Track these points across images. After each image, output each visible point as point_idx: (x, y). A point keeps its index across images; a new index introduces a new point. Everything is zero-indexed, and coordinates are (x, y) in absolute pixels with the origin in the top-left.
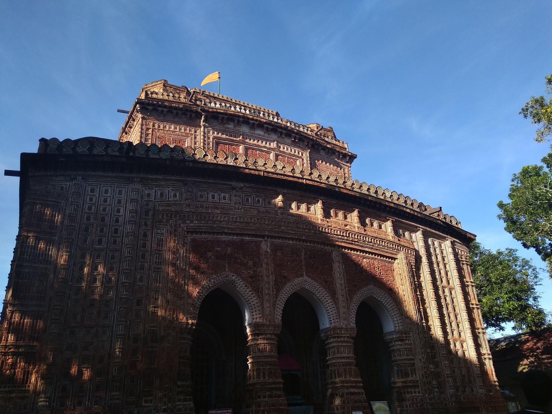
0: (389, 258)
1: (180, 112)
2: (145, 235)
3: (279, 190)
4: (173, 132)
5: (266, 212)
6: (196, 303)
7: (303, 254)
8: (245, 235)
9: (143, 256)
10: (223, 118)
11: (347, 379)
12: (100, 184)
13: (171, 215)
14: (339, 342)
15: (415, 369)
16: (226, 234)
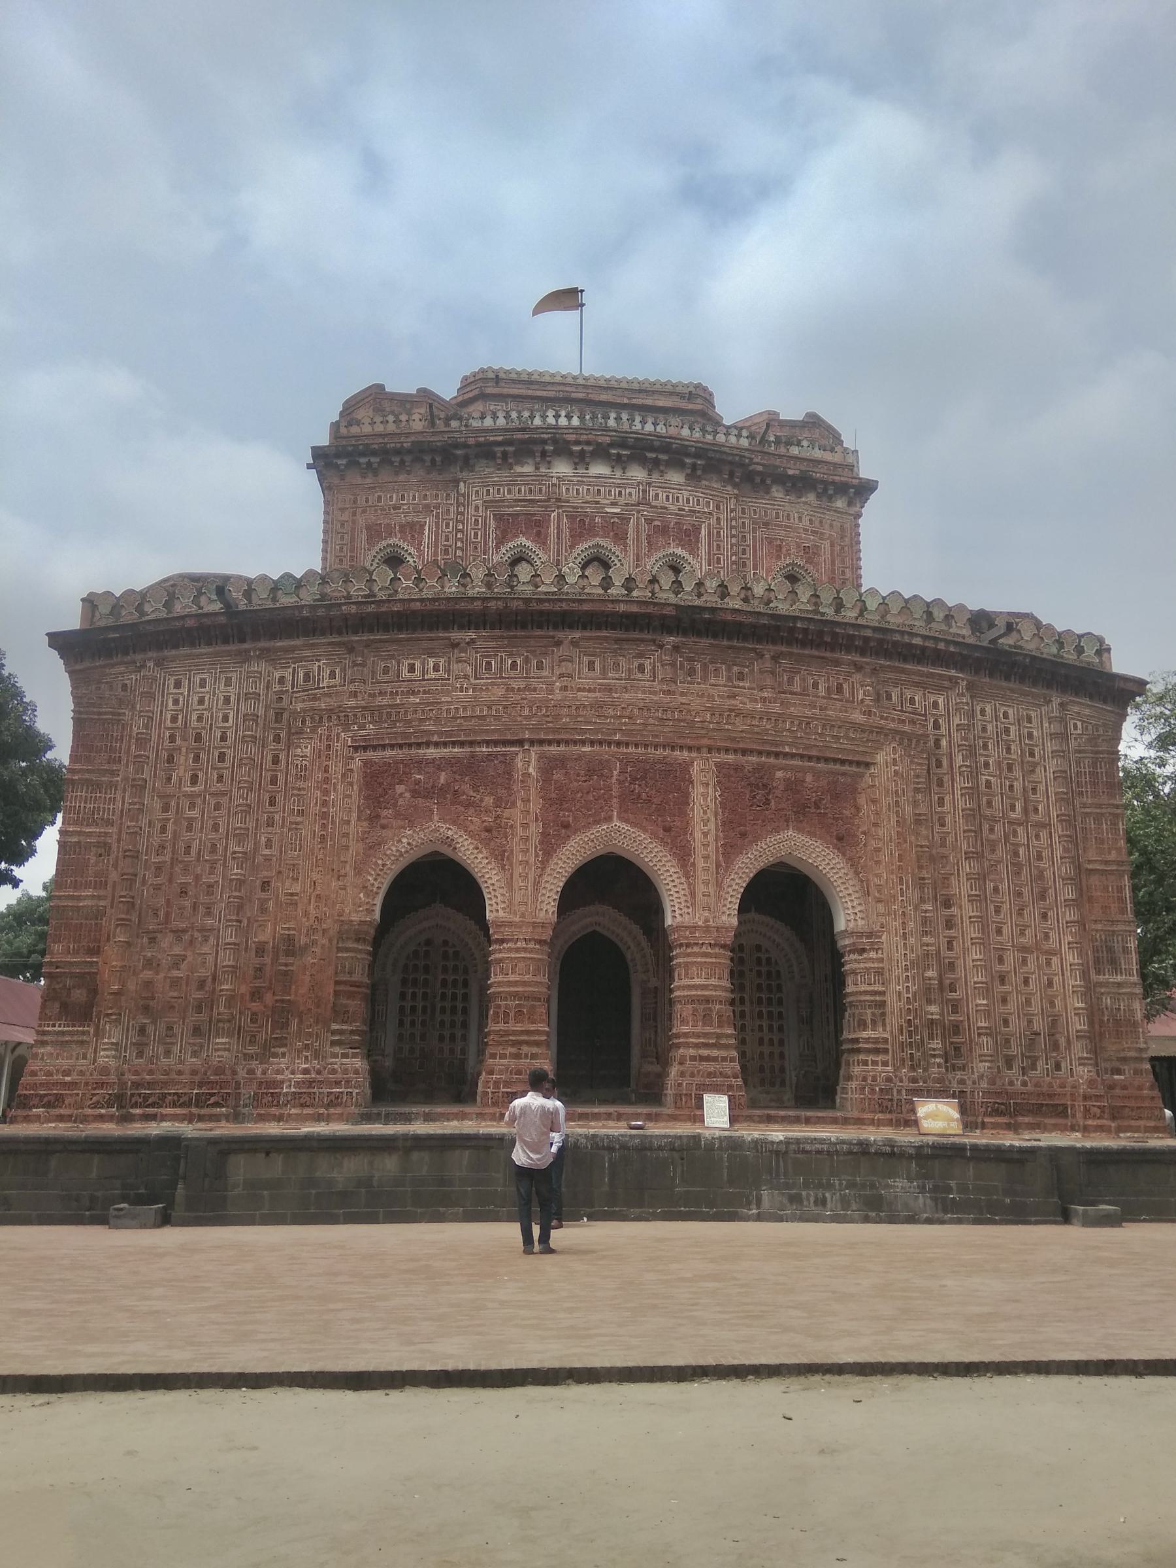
0: (851, 762)
1: (408, 458)
2: (276, 760)
3: (560, 635)
4: (396, 508)
6: (373, 885)
7: (615, 773)
8: (479, 743)
9: (272, 802)
10: (505, 455)
11: (698, 1029)
12: (190, 671)
13: (321, 718)
14: (689, 955)
15: (883, 1014)
16: (437, 745)
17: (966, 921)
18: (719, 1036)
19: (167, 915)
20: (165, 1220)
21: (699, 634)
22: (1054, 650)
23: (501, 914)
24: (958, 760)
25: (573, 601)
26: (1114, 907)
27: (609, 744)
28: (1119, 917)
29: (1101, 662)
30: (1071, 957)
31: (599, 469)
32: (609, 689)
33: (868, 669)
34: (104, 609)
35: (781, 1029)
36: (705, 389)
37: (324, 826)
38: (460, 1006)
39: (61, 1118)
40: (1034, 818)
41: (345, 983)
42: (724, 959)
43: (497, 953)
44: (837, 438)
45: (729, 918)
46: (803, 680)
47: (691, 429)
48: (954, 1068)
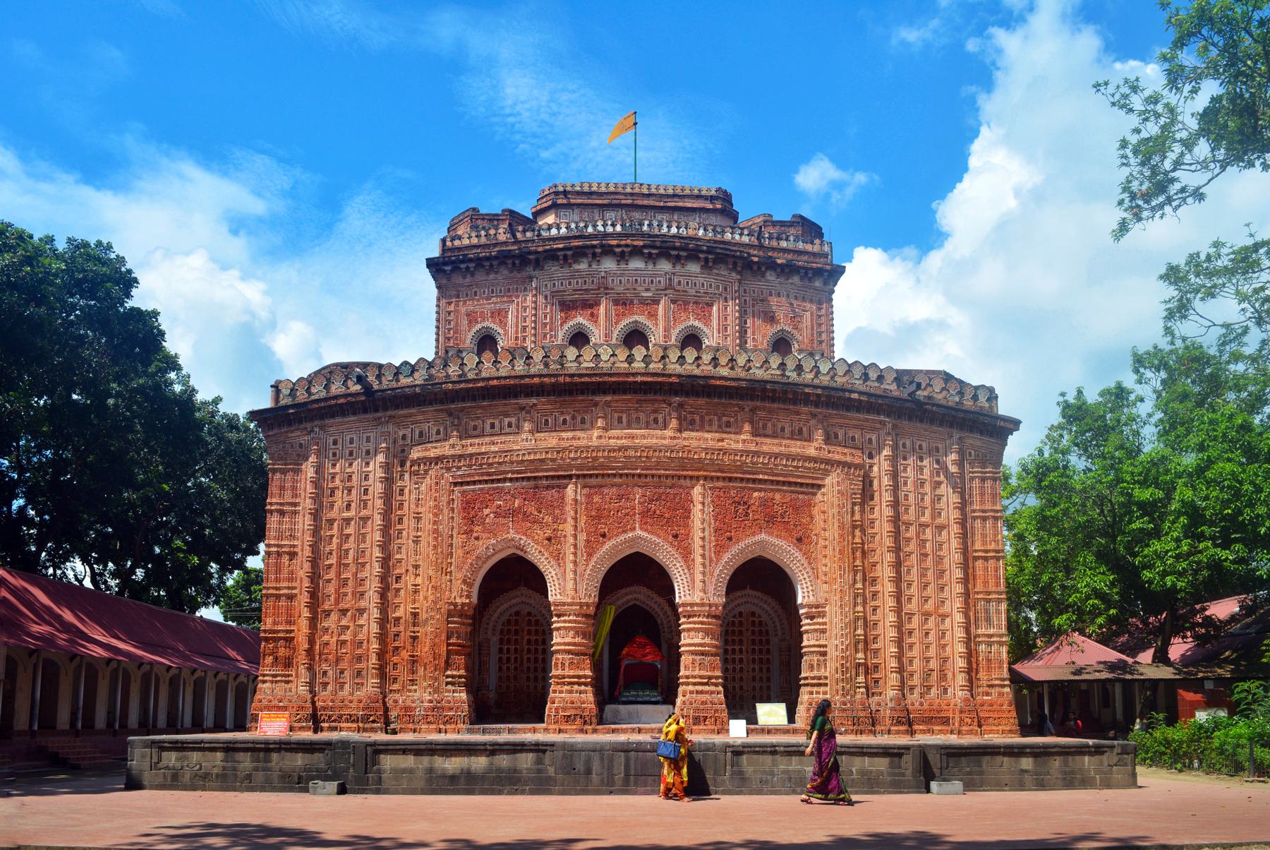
0: (807, 485)
1: (495, 263)
3: (597, 398)
5: (573, 438)
10: (565, 257)
11: (696, 673)
16: (511, 480)
17: (887, 594)
18: (710, 678)
21: (698, 395)
25: (605, 375)
26: (992, 582)
28: (994, 589)
31: (636, 264)
33: (820, 417)
40: (938, 521)
41: (453, 644)
46: (774, 426)
47: (705, 230)
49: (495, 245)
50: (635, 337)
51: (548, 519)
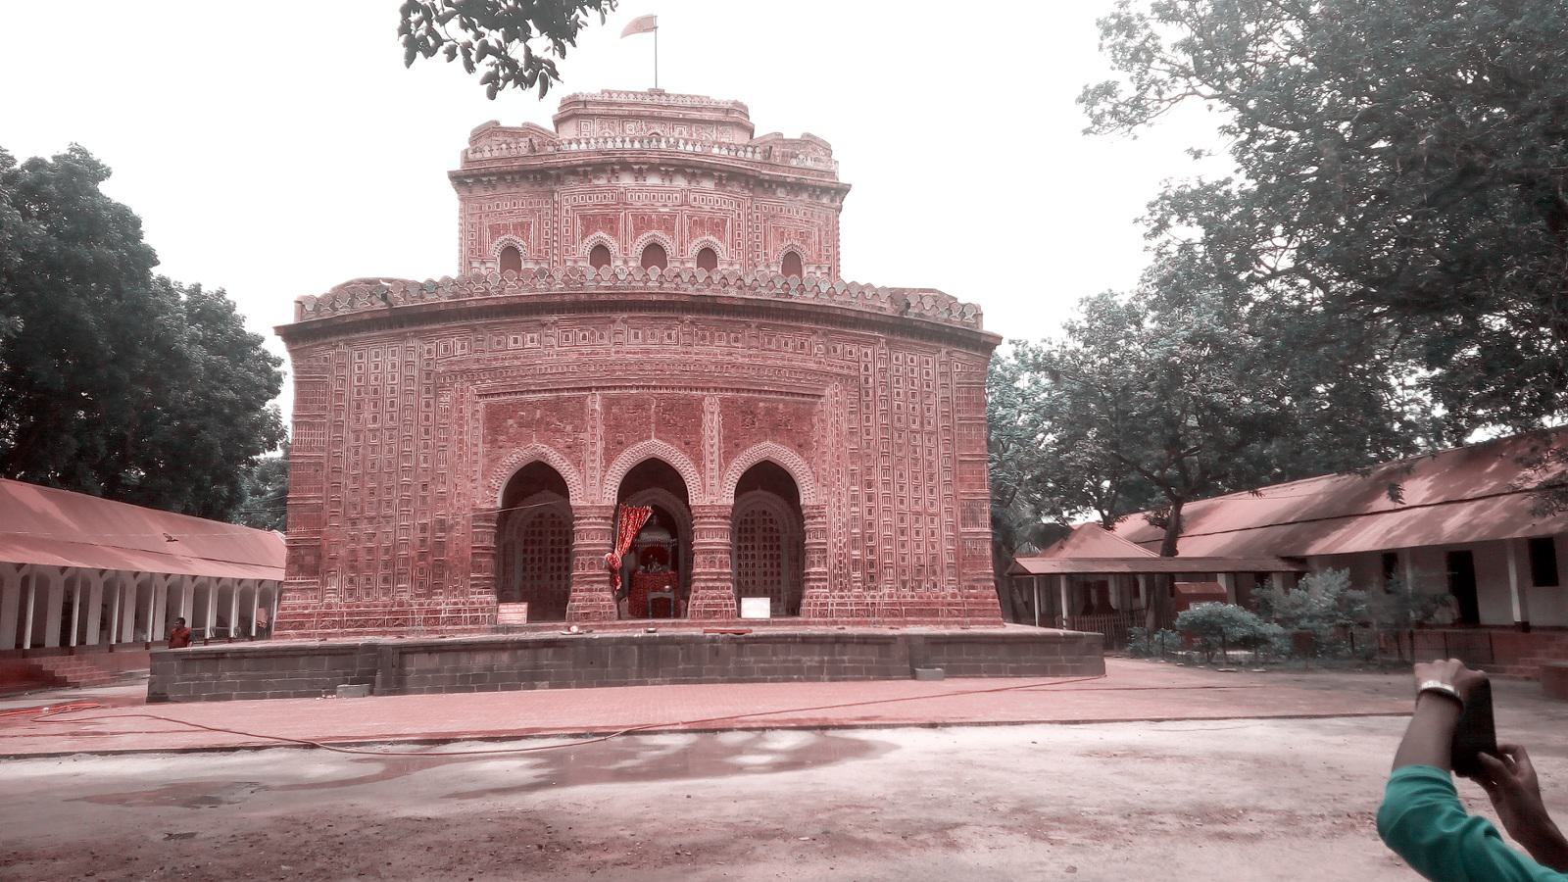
1: (517, 177)
3: (614, 316)
9: (427, 432)
16: (534, 392)
17: (880, 496)
18: (719, 574)
19: (362, 508)
20: (371, 693)
22: (946, 316)
23: (579, 501)
24: (880, 393)
27: (649, 387)
29: (977, 323)
30: (946, 518)
31: (653, 180)
32: (647, 352)
34: (309, 308)
35: (779, 565)
36: (741, 105)
37: (461, 449)
38: (563, 556)
39: (303, 635)
42: (726, 525)
43: (578, 526)
44: (828, 150)
45: (729, 500)
46: (778, 341)
47: (720, 148)
48: (869, 588)
49: (516, 158)
50: (654, 254)
51: (569, 428)
